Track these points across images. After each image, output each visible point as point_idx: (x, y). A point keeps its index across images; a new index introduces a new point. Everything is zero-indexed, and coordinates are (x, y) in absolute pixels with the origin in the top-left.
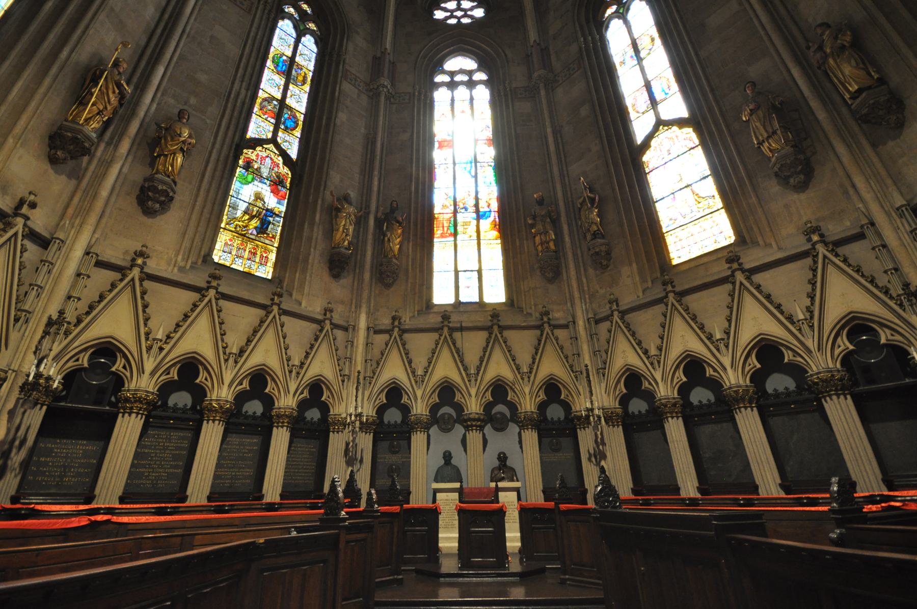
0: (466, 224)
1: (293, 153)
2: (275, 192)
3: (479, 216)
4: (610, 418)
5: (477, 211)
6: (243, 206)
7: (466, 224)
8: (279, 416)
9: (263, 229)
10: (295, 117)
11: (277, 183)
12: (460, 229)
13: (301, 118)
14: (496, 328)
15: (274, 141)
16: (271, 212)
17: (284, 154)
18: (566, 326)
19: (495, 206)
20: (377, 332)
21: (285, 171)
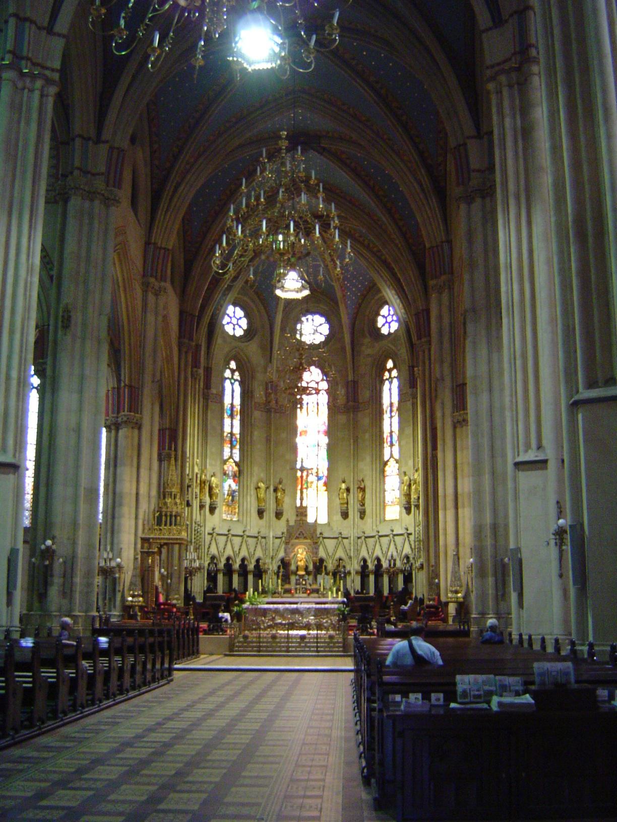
0: (312, 482)
1: (237, 459)
2: (234, 481)
3: (319, 479)
4: (357, 573)
5: (317, 476)
6: (226, 492)
7: (312, 482)
8: (250, 571)
9: (233, 500)
10: (236, 438)
11: (234, 476)
12: (309, 485)
13: (238, 436)
14: (321, 538)
15: (231, 457)
16: (234, 491)
17: (235, 462)
18: (347, 538)
19: (326, 473)
20: (277, 538)
21: (236, 468)
